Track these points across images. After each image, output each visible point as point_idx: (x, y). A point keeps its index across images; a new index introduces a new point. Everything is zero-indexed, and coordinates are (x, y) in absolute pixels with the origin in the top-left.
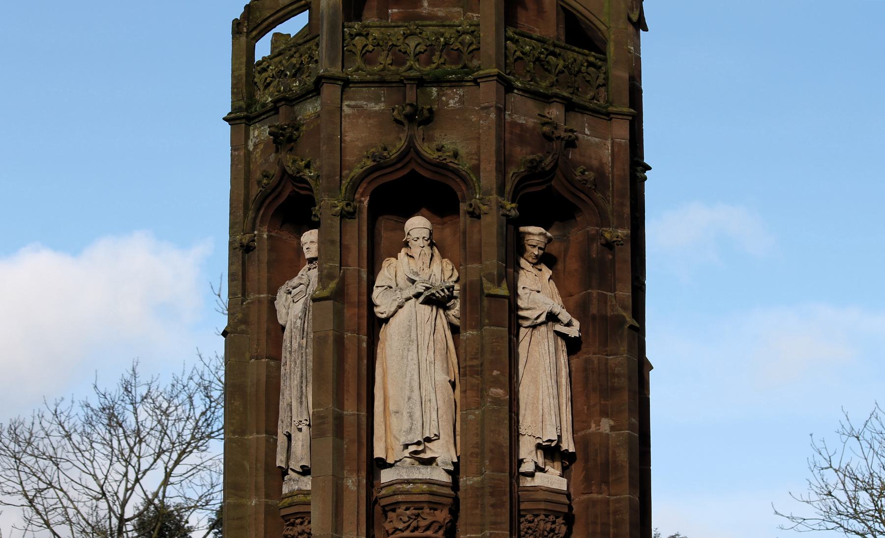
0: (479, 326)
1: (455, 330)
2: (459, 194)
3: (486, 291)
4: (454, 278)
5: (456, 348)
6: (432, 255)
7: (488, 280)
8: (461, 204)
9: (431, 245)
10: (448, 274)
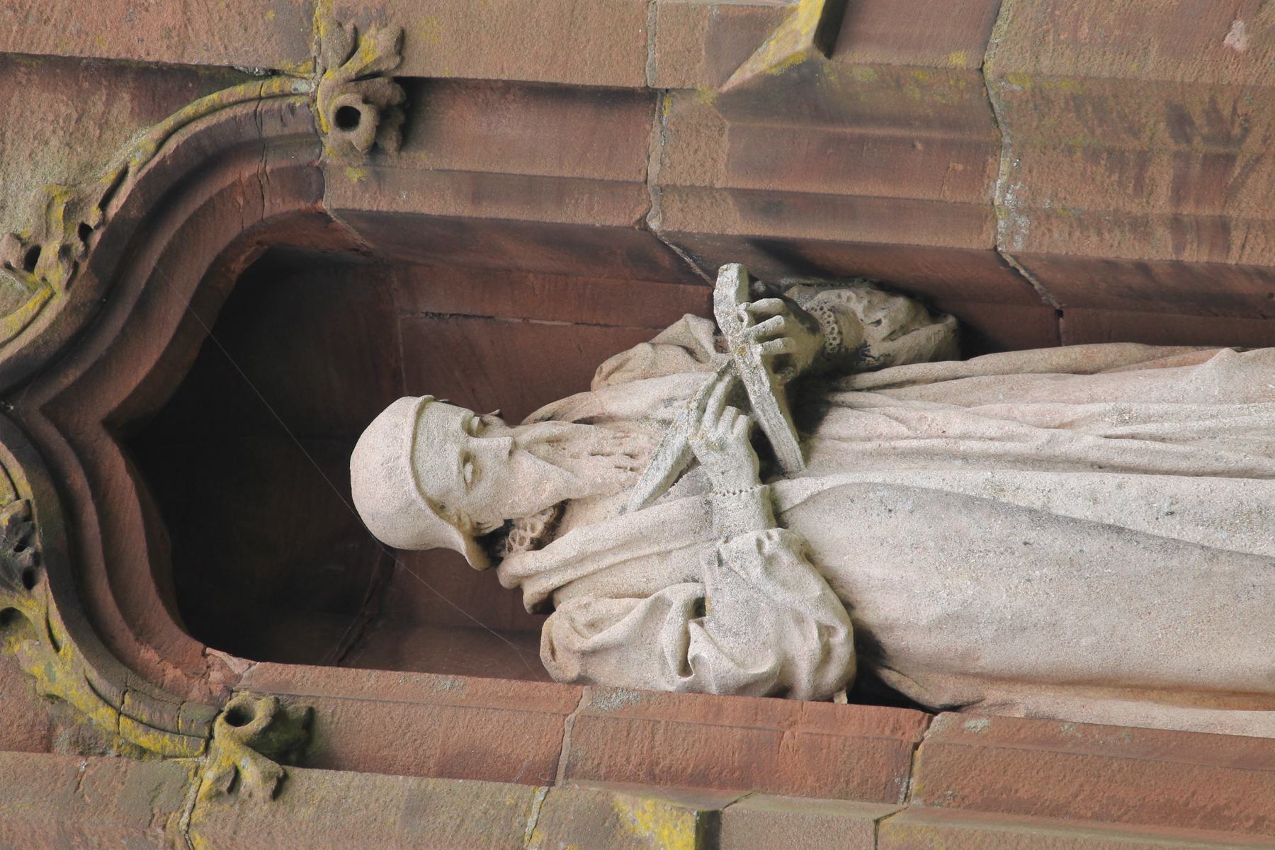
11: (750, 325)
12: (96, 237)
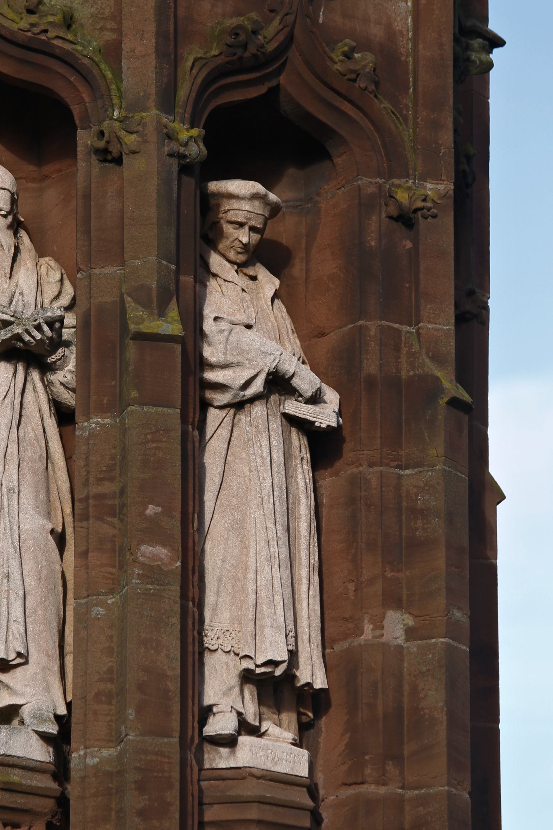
0: (117, 405)
1: (64, 416)
2: (76, 111)
3: (132, 327)
4: (65, 301)
5: (68, 458)
6: (17, 250)
8: (80, 132)
9: (15, 227)
10: (50, 291)
11: (32, 325)
12: (43, 37)
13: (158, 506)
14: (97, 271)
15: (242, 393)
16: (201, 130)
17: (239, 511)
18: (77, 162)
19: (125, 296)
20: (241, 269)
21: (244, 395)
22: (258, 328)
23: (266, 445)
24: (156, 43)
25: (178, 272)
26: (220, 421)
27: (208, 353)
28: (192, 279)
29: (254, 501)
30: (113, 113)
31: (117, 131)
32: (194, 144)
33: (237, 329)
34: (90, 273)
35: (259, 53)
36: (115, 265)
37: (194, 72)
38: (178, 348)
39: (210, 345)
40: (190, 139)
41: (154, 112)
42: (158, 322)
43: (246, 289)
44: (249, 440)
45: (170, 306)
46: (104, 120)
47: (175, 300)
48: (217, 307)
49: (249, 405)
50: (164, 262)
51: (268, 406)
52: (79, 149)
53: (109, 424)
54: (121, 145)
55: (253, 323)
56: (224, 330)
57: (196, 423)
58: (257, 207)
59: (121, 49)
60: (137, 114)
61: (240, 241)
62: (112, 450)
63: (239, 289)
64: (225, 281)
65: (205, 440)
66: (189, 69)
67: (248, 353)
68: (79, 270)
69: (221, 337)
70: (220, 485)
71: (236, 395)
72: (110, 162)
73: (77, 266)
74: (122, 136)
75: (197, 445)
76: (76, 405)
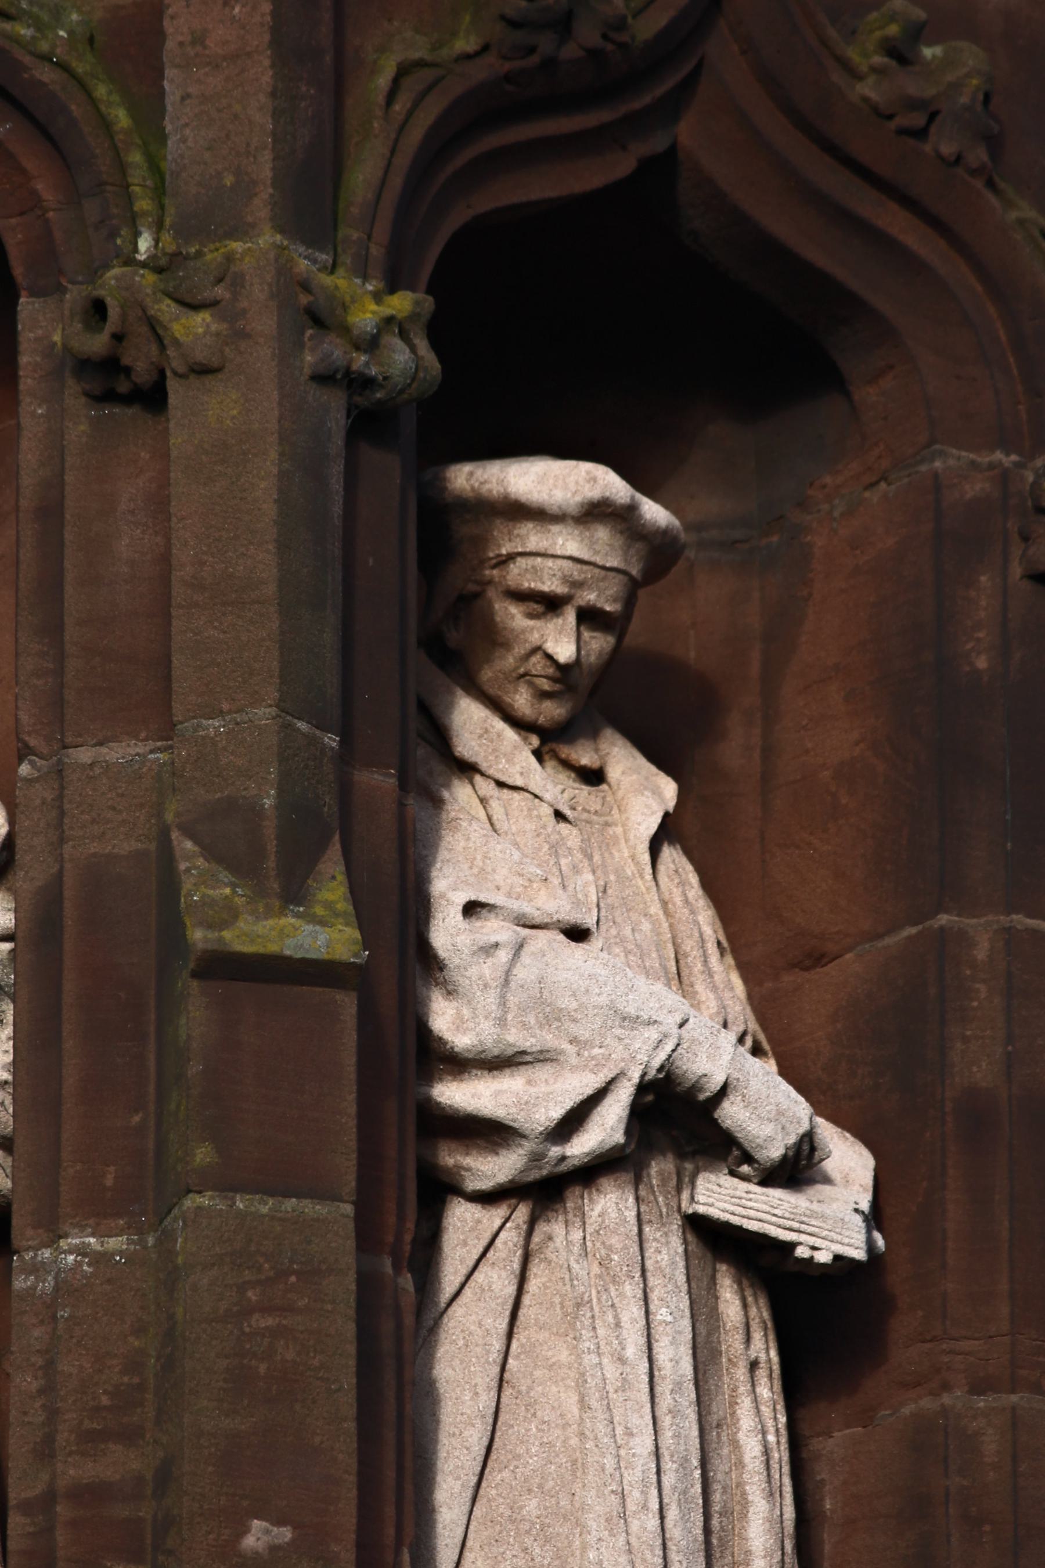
3: (198, 936)
7: (210, 851)
13: (279, 1523)
14: (84, 755)
15: (555, 1151)
16: (420, 296)
17: (547, 1541)
18: (16, 402)
19: (175, 835)
20: (554, 746)
21: (563, 1158)
22: (607, 939)
23: (633, 1321)
24: (274, 14)
25: (347, 755)
26: (484, 1242)
27: (449, 1021)
28: (393, 781)
29: (598, 1506)
30: (136, 244)
31: (148, 301)
32: (398, 343)
33: (542, 939)
34: (60, 761)
35: (610, 47)
36: (143, 735)
37: (397, 107)
38: (347, 1004)
39: (451, 993)
40: (386, 324)
41: (268, 239)
42: (283, 921)
43: (568, 813)
44: (578, 1305)
45: (321, 866)
46: (107, 267)
47: (338, 846)
48: (475, 871)
49: (577, 1190)
50: (302, 725)
51: (642, 1193)
52: (24, 360)
53: (121, 1253)
54: (162, 347)
55: (590, 921)
56: (496, 945)
57: (408, 1248)
58: (600, 546)
59: (160, 35)
60: (212, 246)
61: (549, 657)
62: (131, 1339)
63: (547, 811)
64: (501, 784)
65: (437, 1304)
66: (381, 99)
67: (575, 1020)
68: (24, 753)
69: (489, 969)
70: (483, 1452)
71: (536, 1158)
72: (127, 400)
73: (19, 740)
74: (165, 318)
75: (409, 1320)
76: (13, 1191)
